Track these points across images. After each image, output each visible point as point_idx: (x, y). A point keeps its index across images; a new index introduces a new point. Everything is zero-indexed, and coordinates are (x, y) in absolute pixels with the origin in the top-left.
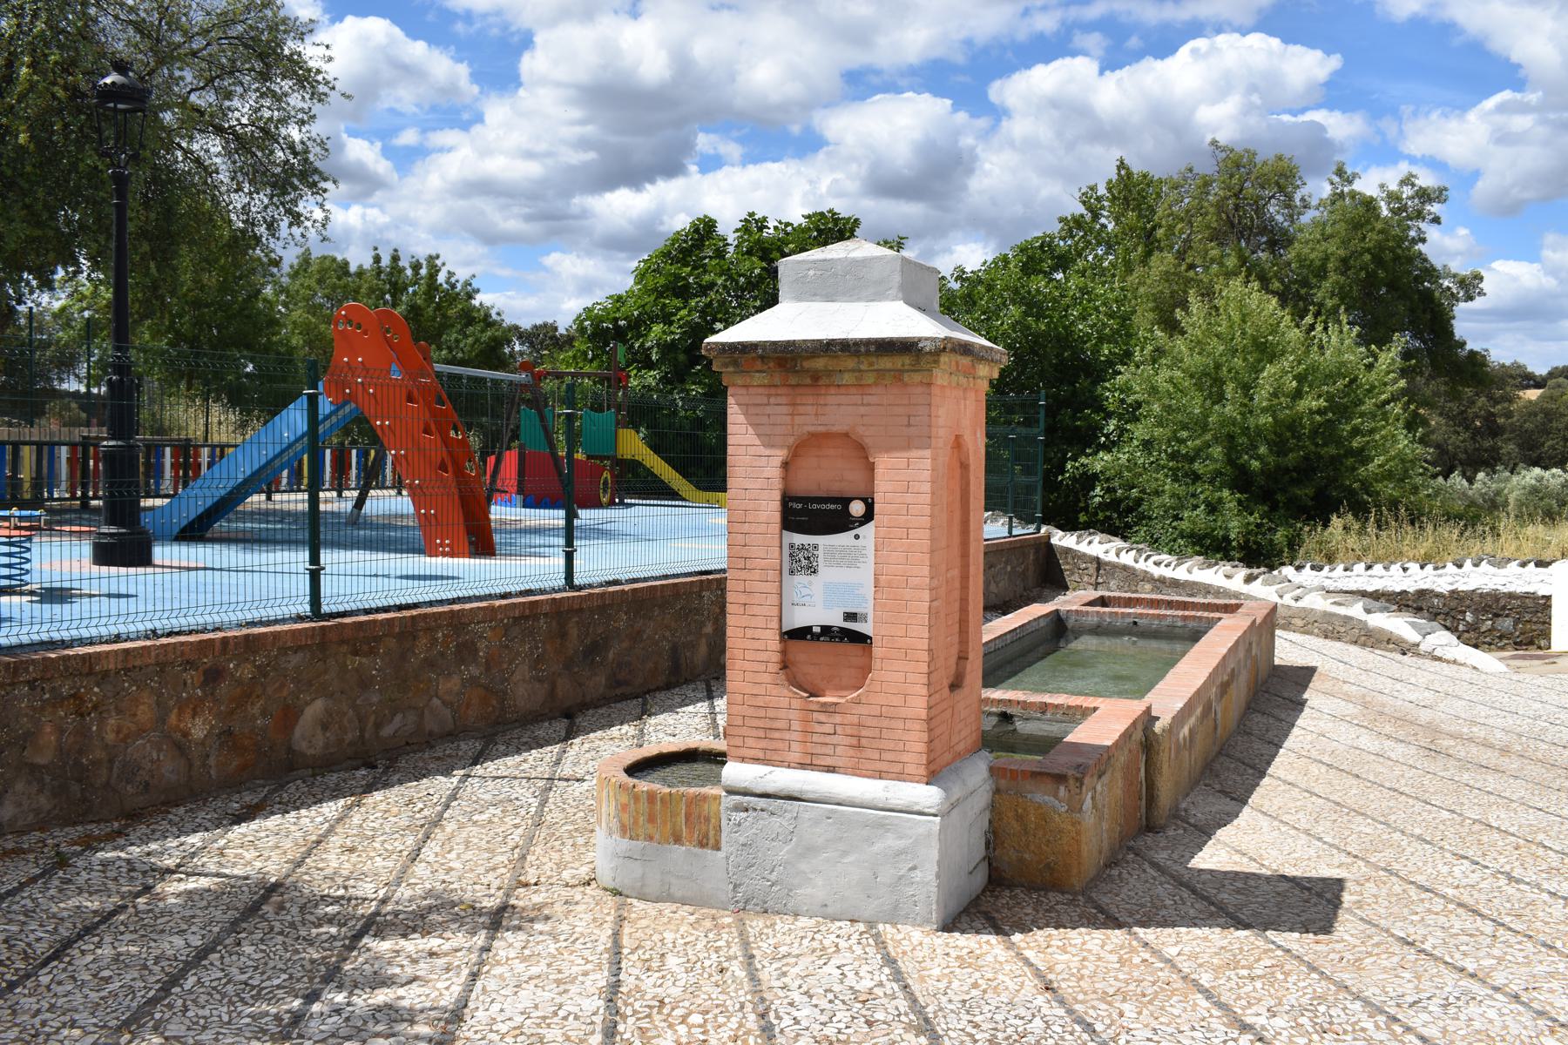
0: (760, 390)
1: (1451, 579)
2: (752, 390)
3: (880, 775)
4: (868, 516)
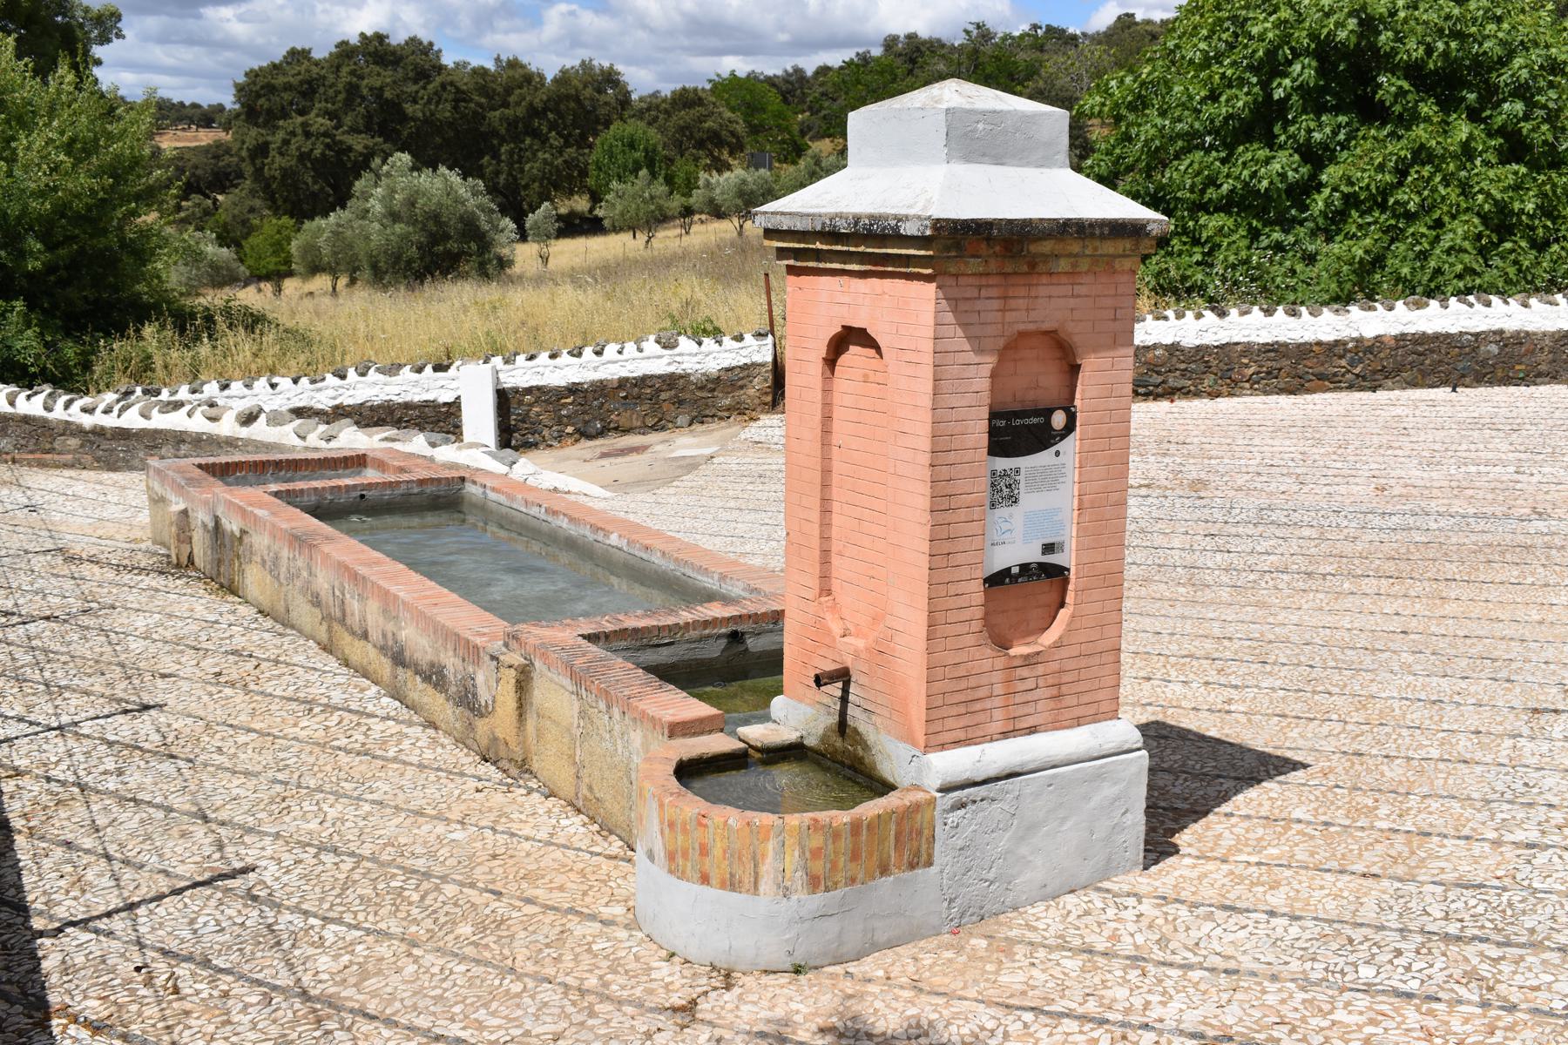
0: (971, 280)
1: (331, 393)
2: (962, 280)
3: (1078, 722)
4: (1070, 427)
